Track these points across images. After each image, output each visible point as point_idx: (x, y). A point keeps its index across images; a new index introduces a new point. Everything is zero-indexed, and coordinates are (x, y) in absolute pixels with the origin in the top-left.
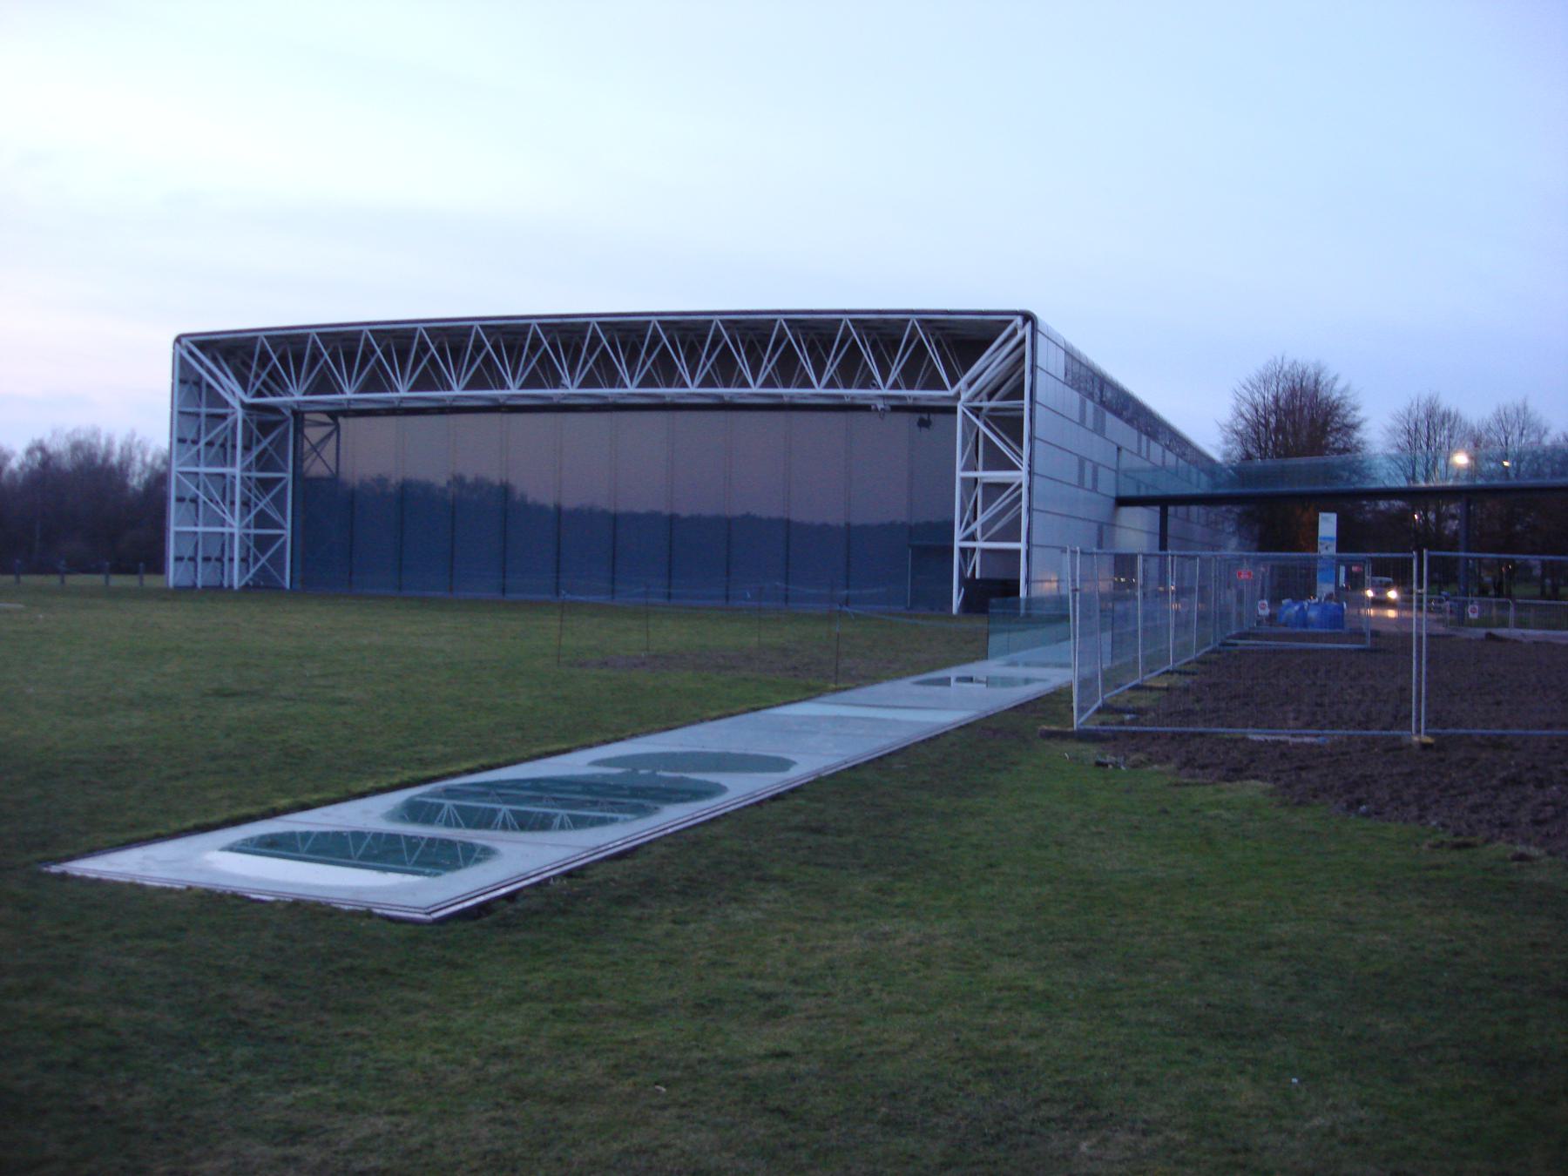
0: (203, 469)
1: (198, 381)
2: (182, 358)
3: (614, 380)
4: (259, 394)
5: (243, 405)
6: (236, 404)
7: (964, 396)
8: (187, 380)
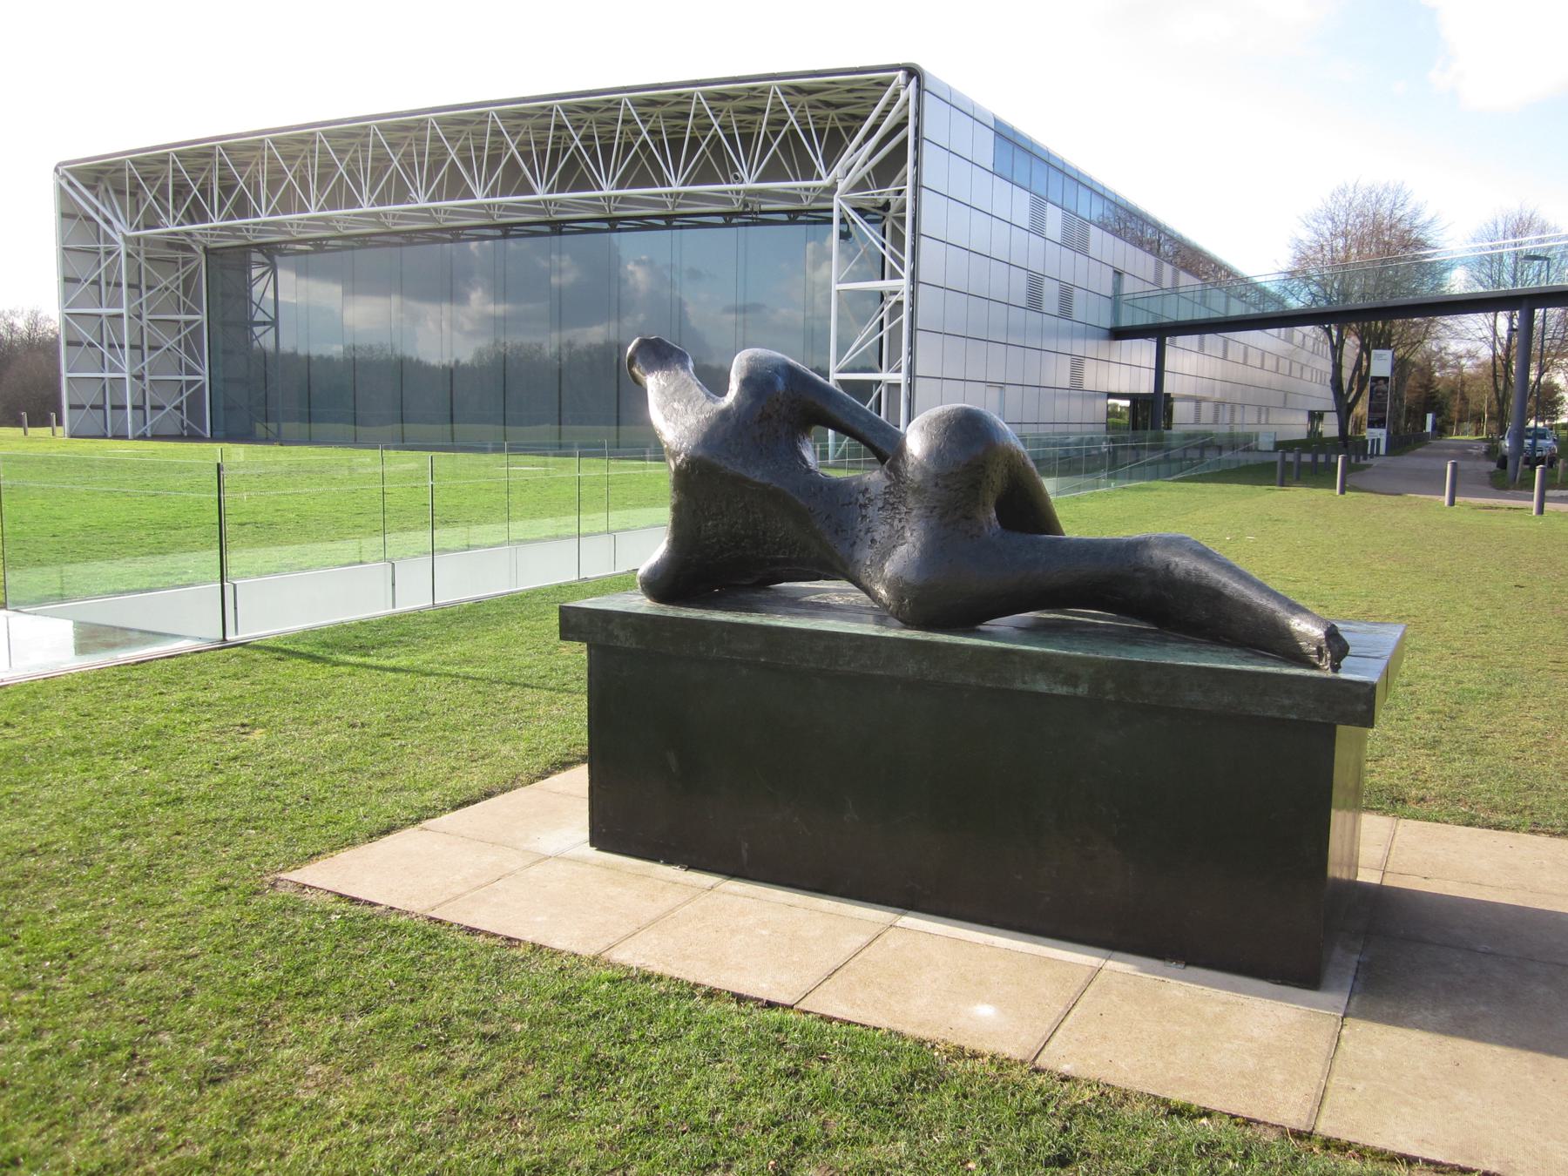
0: (104, 311)
1: (89, 219)
2: (61, 189)
5: (126, 239)
7: (841, 186)
8: (69, 214)
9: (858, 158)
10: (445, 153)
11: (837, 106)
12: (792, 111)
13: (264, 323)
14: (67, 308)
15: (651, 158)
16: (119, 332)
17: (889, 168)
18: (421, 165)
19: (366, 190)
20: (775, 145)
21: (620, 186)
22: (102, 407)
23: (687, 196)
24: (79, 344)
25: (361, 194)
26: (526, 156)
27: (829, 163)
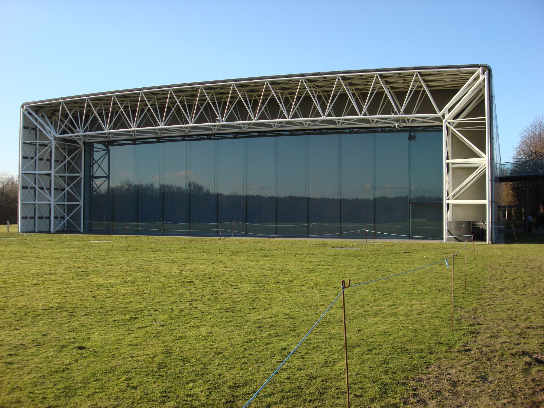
1: (35, 129)
2: (24, 115)
4: (64, 132)
5: (55, 138)
6: (52, 138)
11: (288, 89)
12: (208, 96)
14: (24, 170)
15: (151, 115)
20: (202, 109)
22: (49, 218)
23: (166, 130)
26: (100, 115)
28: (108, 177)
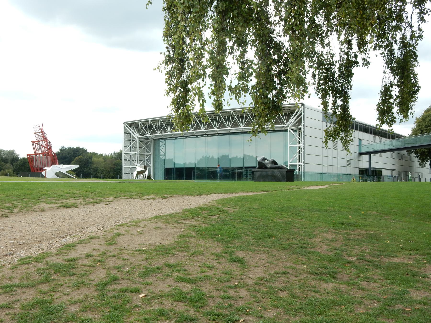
0: (131, 153)
1: (130, 133)
3: (224, 126)
5: (138, 138)
6: (136, 138)
7: (289, 126)
8: (126, 133)
9: (293, 120)
10: (221, 119)
13: (163, 155)
16: (135, 158)
17: (299, 122)
18: (169, 124)
19: (158, 130)
21: (231, 127)
24: (126, 160)
25: (157, 131)
27: (287, 122)
28: (165, 155)
